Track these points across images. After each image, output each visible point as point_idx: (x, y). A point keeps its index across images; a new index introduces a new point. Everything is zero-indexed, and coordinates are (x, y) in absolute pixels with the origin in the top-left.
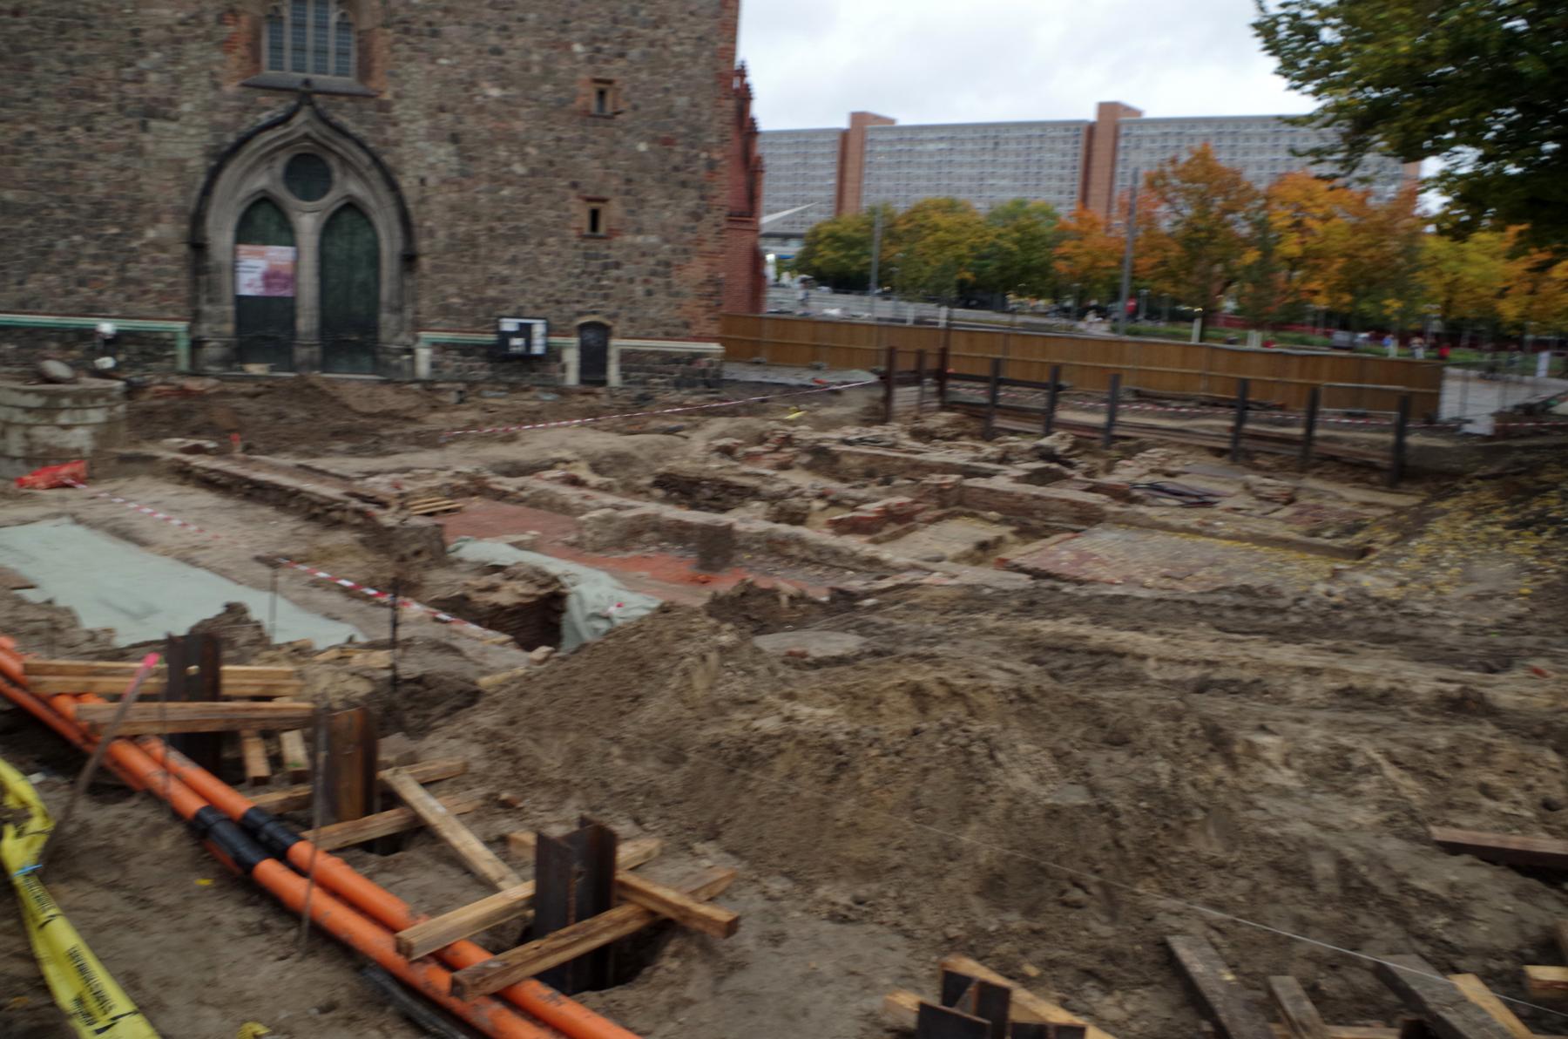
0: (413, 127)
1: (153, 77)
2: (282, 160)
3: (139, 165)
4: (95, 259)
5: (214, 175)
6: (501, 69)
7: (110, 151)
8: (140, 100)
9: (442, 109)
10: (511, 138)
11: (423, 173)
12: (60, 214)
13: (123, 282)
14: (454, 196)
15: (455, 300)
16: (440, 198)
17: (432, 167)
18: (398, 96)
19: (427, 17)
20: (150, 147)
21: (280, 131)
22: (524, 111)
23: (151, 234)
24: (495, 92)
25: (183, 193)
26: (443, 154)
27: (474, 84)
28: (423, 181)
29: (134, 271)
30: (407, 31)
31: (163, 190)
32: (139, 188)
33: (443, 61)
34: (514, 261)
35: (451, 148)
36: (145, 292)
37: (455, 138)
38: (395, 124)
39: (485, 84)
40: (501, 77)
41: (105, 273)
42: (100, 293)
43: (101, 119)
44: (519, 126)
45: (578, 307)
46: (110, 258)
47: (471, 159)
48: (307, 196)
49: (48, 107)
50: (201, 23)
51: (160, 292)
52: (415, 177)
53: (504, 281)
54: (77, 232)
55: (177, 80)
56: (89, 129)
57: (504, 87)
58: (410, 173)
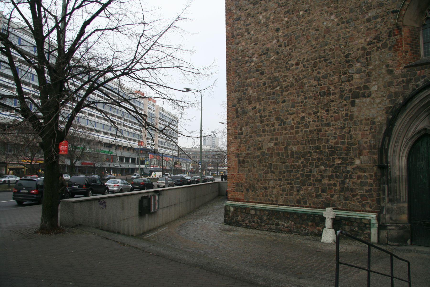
1: (356, 76)
5: (391, 124)
8: (350, 90)
20: (356, 114)
23: (357, 162)
25: (374, 137)
29: (349, 183)
32: (351, 137)
36: (354, 196)
41: (335, 185)
46: (337, 176)
49: (310, 102)
50: (379, 41)
51: (362, 196)
54: (322, 164)
55: (369, 74)
56: (327, 111)
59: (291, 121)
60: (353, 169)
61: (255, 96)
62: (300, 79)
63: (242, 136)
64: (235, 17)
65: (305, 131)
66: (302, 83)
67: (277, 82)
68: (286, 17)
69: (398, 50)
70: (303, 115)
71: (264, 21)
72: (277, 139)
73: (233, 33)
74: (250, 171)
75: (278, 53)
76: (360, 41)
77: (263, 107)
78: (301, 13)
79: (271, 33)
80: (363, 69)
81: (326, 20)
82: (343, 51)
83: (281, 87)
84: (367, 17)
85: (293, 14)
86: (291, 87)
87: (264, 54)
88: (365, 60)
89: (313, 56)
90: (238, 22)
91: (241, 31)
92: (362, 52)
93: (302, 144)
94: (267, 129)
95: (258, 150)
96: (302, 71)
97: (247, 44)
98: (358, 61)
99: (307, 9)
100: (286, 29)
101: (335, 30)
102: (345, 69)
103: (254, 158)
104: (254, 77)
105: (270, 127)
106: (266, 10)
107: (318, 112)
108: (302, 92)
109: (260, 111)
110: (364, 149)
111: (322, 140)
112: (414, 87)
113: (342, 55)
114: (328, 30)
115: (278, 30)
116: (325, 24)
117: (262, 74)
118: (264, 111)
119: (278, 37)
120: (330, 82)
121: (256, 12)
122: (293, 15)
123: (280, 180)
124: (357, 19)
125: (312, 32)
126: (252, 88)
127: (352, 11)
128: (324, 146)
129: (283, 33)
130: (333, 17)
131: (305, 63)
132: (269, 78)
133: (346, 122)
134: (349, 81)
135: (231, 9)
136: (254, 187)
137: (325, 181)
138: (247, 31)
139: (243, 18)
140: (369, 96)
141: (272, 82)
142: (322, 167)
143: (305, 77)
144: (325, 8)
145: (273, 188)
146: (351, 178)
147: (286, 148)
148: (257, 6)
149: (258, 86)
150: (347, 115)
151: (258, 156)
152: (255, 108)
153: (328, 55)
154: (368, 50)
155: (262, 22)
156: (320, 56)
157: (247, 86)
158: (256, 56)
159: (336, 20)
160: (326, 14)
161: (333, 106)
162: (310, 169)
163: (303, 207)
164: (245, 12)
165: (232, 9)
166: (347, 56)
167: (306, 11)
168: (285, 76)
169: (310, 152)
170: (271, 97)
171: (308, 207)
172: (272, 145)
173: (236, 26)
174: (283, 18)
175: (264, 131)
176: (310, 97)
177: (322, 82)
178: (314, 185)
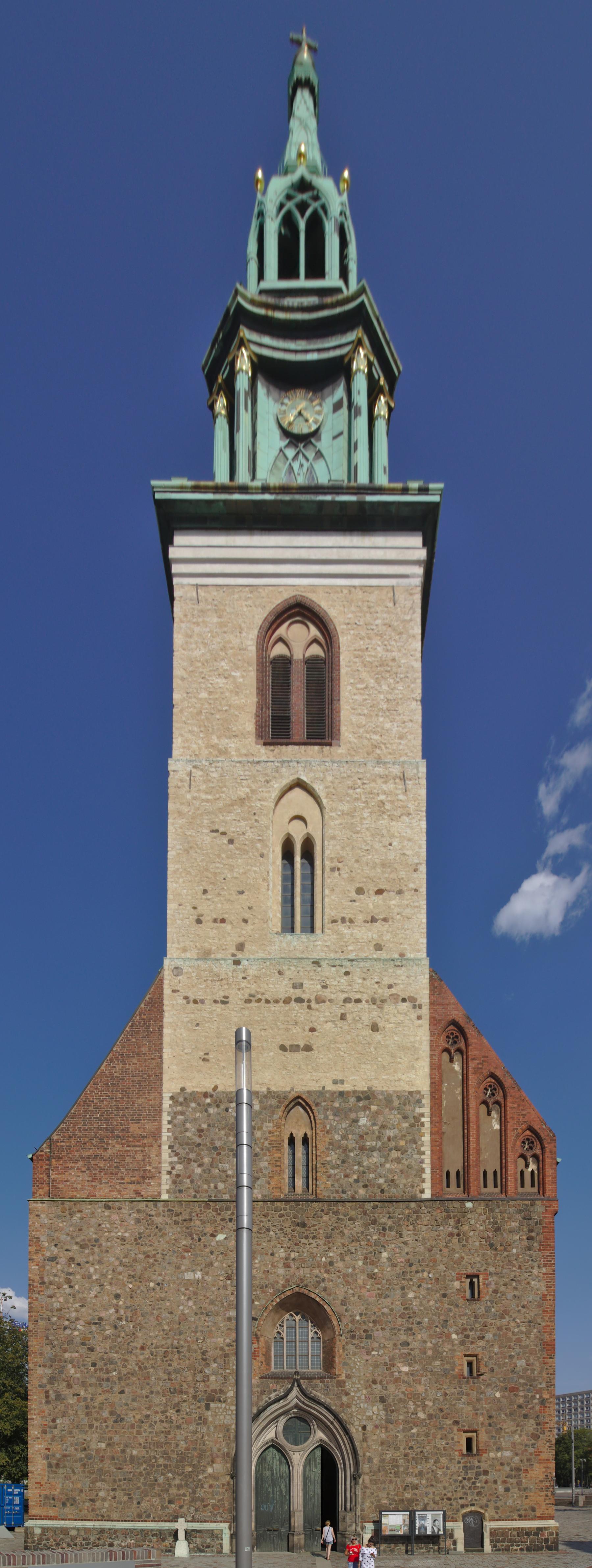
0: (358, 1395)
1: (213, 1378)
2: (282, 1421)
3: (204, 1430)
4: (179, 1487)
6: (409, 1354)
7: (188, 1422)
9: (374, 1382)
10: (415, 1396)
11: (364, 1423)
12: (161, 1461)
13: (194, 1500)
14: (383, 1436)
15: (386, 1501)
16: (375, 1437)
17: (370, 1418)
18: (347, 1376)
19: (364, 1327)
20: (210, 1419)
21: (282, 1403)
22: (423, 1379)
23: (210, 1470)
24: (406, 1369)
26: (376, 1411)
27: (393, 1365)
28: (364, 1428)
29: (200, 1493)
30: (353, 1337)
31: (217, 1443)
33: (374, 1353)
34: (420, 1474)
35: (381, 1406)
37: (382, 1400)
38: (347, 1394)
39: (399, 1365)
40: (408, 1359)
41: (184, 1495)
42: (181, 1507)
43: (184, 1404)
44: (421, 1389)
45: (461, 1502)
47: (393, 1411)
48: (296, 1443)
49: (157, 1400)
51: (214, 1506)
52: (359, 1426)
53: (416, 1487)
54: (170, 1471)
56: (178, 1411)
57: (410, 1365)
58: (357, 1423)
59: (131, 1418)
60: (205, 1478)
61: (78, 1379)
62: (146, 1368)
63: (56, 1432)
64: (48, 1254)
65: (150, 1432)
66: (148, 1373)
67: (112, 1366)
68: (131, 1283)
69: (255, 1359)
70: (148, 1413)
71: (98, 1277)
72: (111, 1439)
73: (42, 1278)
74: (67, 1478)
75: (116, 1327)
76: (219, 1339)
77: (90, 1396)
78: (152, 1285)
79: (106, 1298)
80: (221, 1371)
81: (183, 1304)
82: (200, 1346)
83: (119, 1373)
84: (227, 1315)
85: (141, 1282)
86: (133, 1374)
87: (95, 1324)
88: (223, 1363)
89: (163, 1342)
90: (53, 1264)
91: (57, 1279)
92: (221, 1352)
93: (144, 1447)
94: (96, 1424)
95: (82, 1451)
96: (148, 1359)
97: (67, 1302)
98: (215, 1361)
99: (160, 1282)
100: (129, 1299)
101: (193, 1319)
102: (200, 1367)
103: (75, 1461)
104: (77, 1352)
105: (101, 1423)
106: (100, 1262)
107: (166, 1411)
108: (148, 1384)
109: (85, 1399)
110: (218, 1456)
111: (171, 1444)
112: (267, 1399)
113: (199, 1351)
114: (184, 1318)
115: (117, 1296)
116: (181, 1308)
117: (91, 1349)
118: (92, 1400)
119: (117, 1306)
120: (183, 1379)
121: (85, 1260)
122: (140, 1284)
123: (114, 1490)
124: (218, 1314)
125: (165, 1314)
126: (74, 1366)
127: (212, 1303)
128: (173, 1451)
129: (124, 1302)
130: (191, 1303)
131: (153, 1350)
132: (102, 1359)
133: (199, 1427)
134: (204, 1381)
135: (39, 1238)
136: (74, 1500)
137: (173, 1491)
138: (68, 1281)
139: (63, 1260)
140: (224, 1402)
141: (106, 1364)
142: (170, 1475)
143: (152, 1367)
144: (183, 1289)
145: (104, 1500)
146: (202, 1487)
147: (123, 1451)
148: (87, 1251)
149: (84, 1365)
150: (200, 1418)
151: (81, 1460)
152: (78, 1395)
153: (183, 1347)
154: (227, 1352)
155: (94, 1277)
156: (172, 1345)
157: (66, 1362)
158: (82, 1322)
159: (194, 1307)
160: (183, 1297)
161: (185, 1407)
162: (155, 1477)
163: (145, 1521)
164: (65, 1252)
165: (42, 1239)
166: (204, 1353)
167: (158, 1284)
168: (126, 1360)
169: (155, 1458)
170: (104, 1384)
171: (152, 1521)
172: (103, 1445)
173: (48, 1268)
174: (126, 1283)
175: (91, 1426)
176: (158, 1393)
177: (173, 1376)
178: (159, 1495)
